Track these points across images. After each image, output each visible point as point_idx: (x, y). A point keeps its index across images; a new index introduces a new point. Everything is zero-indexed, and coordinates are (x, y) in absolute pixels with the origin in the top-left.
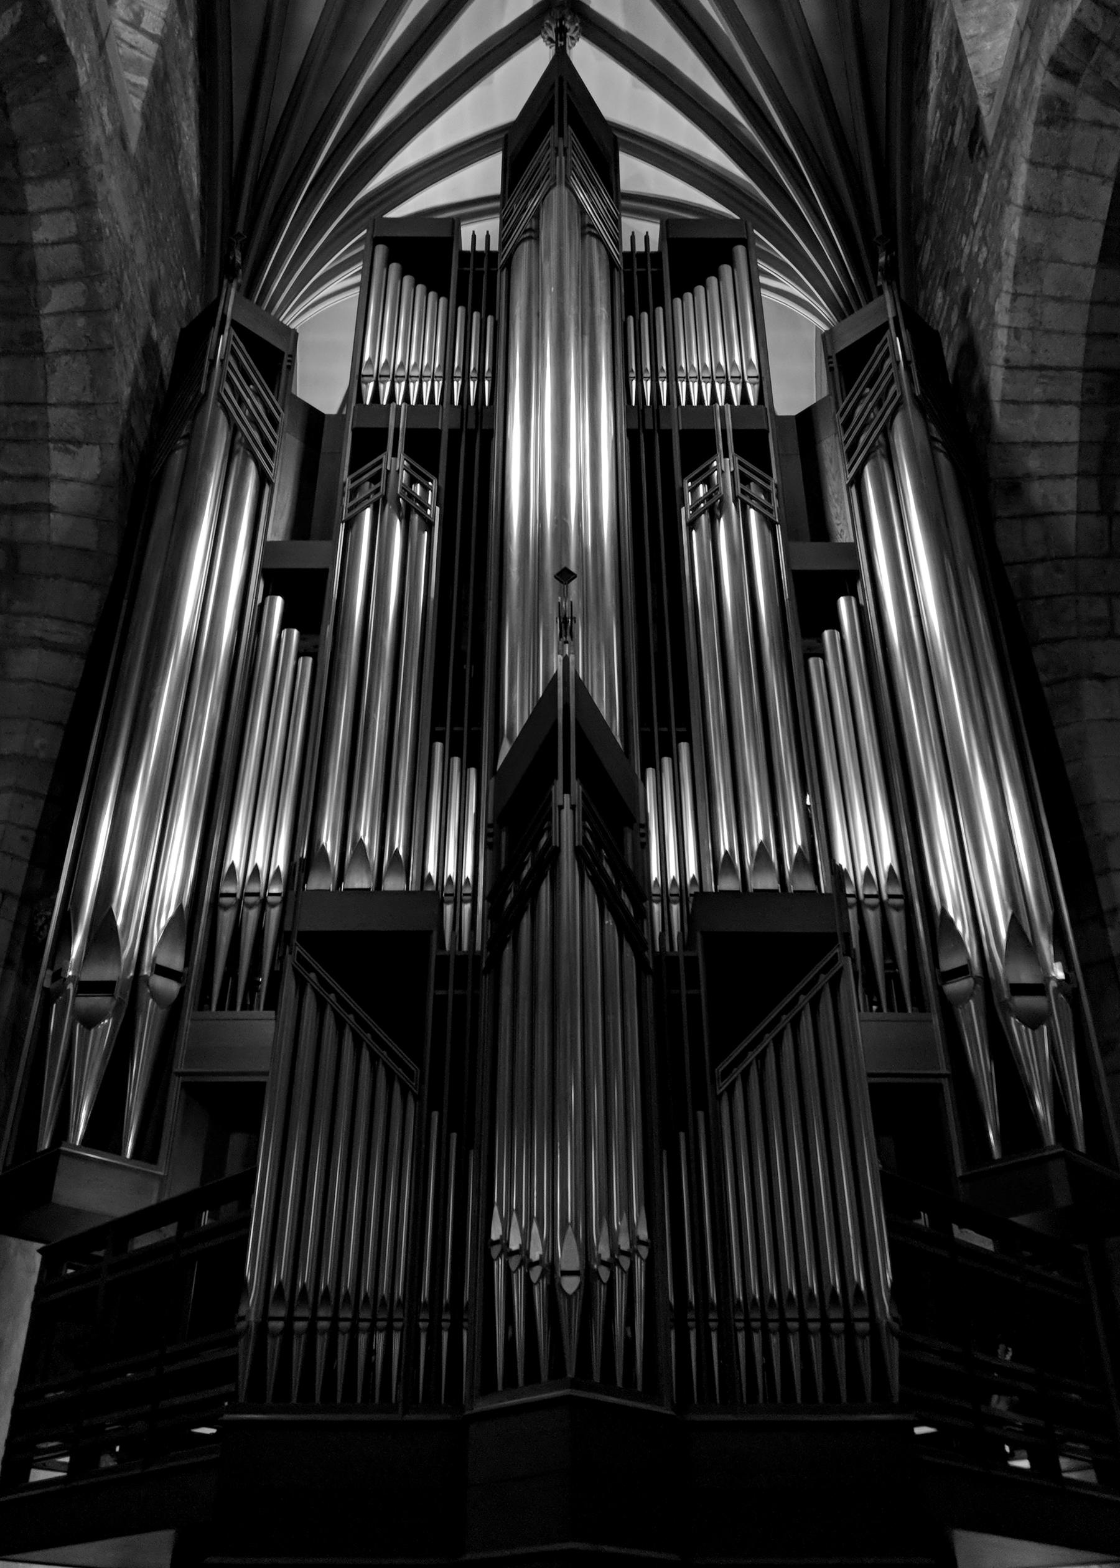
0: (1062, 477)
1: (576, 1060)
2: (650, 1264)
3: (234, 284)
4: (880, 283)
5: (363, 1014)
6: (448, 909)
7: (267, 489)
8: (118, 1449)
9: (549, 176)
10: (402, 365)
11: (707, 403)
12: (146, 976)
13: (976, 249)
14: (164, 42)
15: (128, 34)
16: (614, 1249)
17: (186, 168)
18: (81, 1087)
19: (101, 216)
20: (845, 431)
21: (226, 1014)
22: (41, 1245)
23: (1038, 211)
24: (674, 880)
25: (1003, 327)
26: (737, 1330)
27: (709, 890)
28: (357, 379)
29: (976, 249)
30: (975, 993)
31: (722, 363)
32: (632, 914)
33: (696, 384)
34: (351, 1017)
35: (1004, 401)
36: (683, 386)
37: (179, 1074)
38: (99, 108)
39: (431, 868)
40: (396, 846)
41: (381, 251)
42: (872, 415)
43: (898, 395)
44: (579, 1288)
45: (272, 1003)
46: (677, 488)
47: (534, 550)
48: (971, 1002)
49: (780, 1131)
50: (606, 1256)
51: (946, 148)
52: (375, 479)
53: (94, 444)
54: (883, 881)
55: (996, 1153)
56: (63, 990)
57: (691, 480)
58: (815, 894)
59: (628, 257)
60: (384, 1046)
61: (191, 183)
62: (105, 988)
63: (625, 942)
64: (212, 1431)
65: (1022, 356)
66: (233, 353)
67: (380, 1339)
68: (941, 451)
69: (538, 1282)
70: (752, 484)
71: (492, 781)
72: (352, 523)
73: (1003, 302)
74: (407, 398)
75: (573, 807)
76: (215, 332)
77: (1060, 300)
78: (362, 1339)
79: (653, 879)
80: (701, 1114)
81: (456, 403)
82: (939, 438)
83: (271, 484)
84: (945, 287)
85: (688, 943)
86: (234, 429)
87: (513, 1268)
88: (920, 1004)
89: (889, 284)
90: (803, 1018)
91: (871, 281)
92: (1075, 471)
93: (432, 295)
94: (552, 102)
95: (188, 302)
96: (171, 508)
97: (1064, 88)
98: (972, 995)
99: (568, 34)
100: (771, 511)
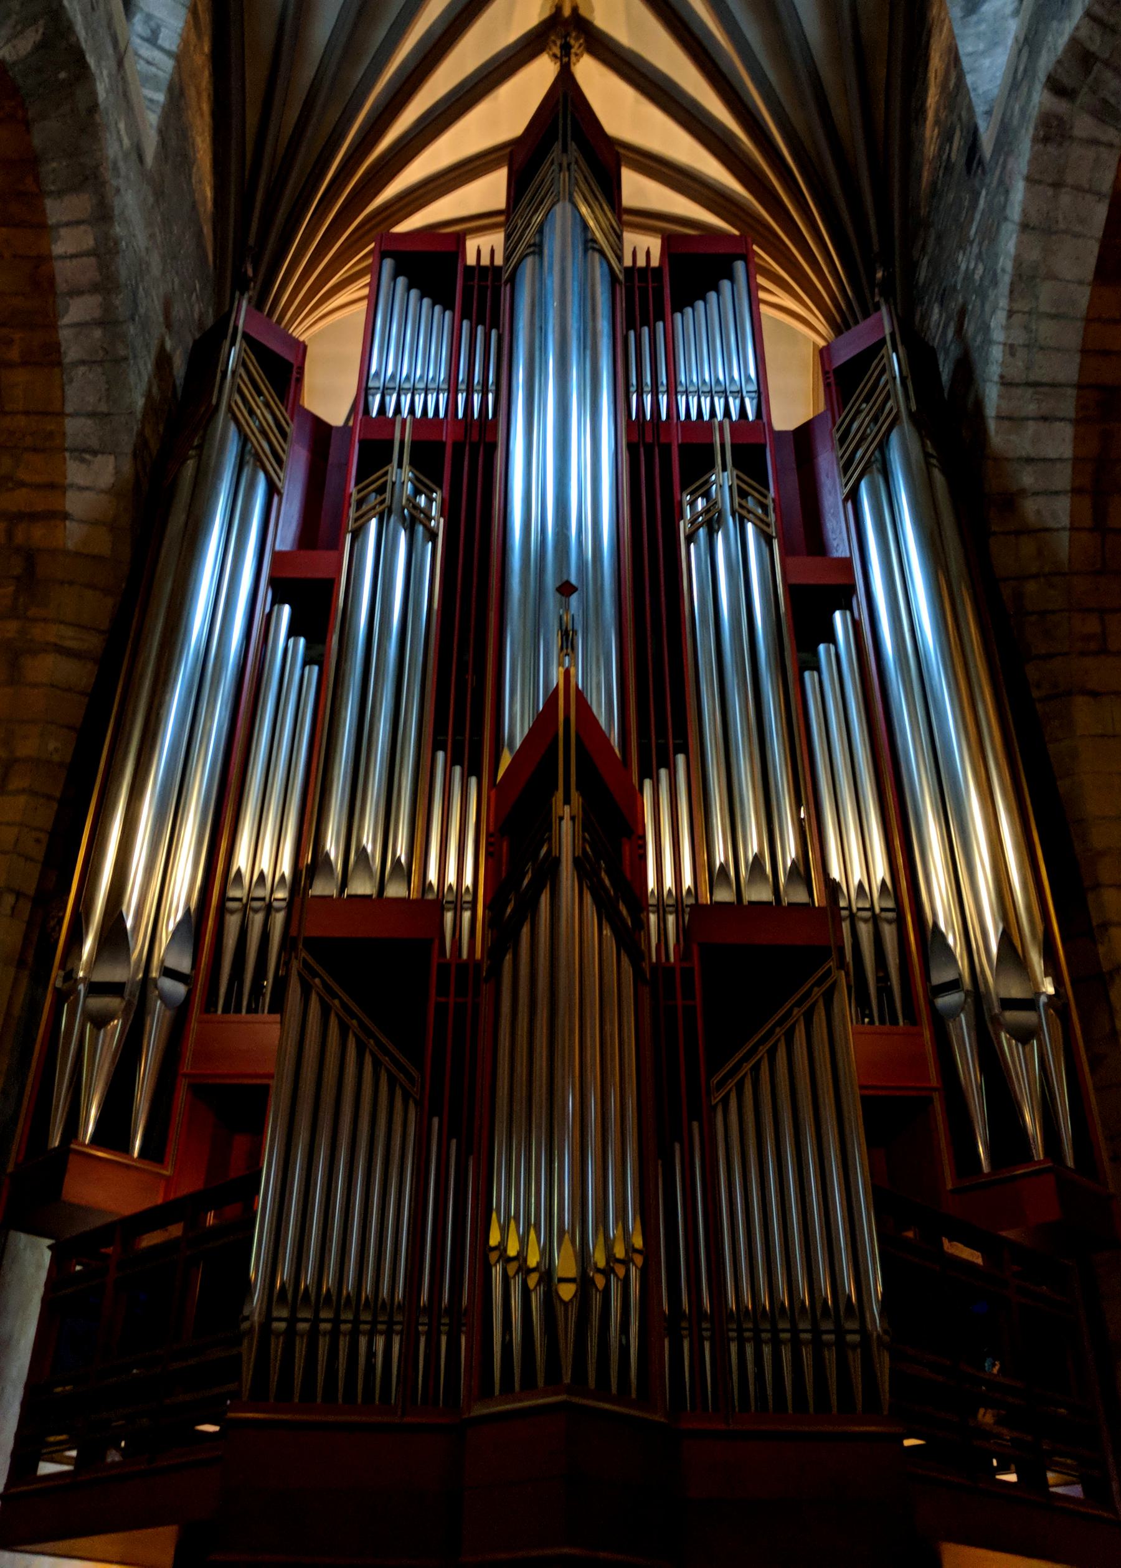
1: (574, 1066)
2: (644, 1272)
3: (246, 296)
4: (877, 299)
5: (367, 1021)
6: (449, 916)
8: (123, 1444)
10: (408, 378)
11: (706, 417)
12: (155, 978)
13: (972, 266)
14: (180, 58)
15: (146, 51)
16: (610, 1256)
17: (200, 182)
18: (90, 1088)
19: (118, 230)
20: (841, 447)
21: (232, 1017)
22: (49, 1242)
24: (670, 891)
25: (999, 343)
26: (730, 1339)
27: (705, 902)
28: (364, 391)
29: (972, 266)
30: (966, 1006)
31: (721, 378)
32: (630, 924)
33: (696, 399)
34: (354, 1022)
35: (999, 418)
36: (682, 401)
37: (186, 1075)
38: (116, 124)
39: (433, 876)
40: (398, 854)
41: (388, 264)
42: (868, 431)
43: (894, 411)
44: (575, 1295)
45: (277, 1006)
46: (675, 501)
47: (535, 565)
48: (962, 1016)
49: (773, 1142)
50: (602, 1264)
51: (944, 164)
52: (381, 490)
54: (876, 894)
56: (74, 991)
57: (691, 494)
58: (808, 907)
59: (629, 271)
60: (387, 1052)
61: (206, 198)
62: (114, 989)
63: (622, 952)
64: (216, 1428)
65: (1017, 371)
66: (244, 365)
67: (380, 1342)
68: (935, 466)
69: (535, 1287)
70: (749, 498)
71: (493, 792)
72: (359, 533)
75: (573, 818)
78: (363, 1341)
79: (650, 890)
80: (695, 1124)
81: (460, 415)
82: (935, 454)
83: (280, 494)
85: (684, 953)
86: (244, 440)
87: (511, 1273)
88: (911, 1016)
89: (887, 301)
90: (797, 1031)
91: (868, 296)
92: (1069, 488)
93: (437, 308)
95: (201, 315)
96: (183, 517)
97: (1062, 106)
98: (963, 1009)
99: (573, 51)
100: (768, 525)
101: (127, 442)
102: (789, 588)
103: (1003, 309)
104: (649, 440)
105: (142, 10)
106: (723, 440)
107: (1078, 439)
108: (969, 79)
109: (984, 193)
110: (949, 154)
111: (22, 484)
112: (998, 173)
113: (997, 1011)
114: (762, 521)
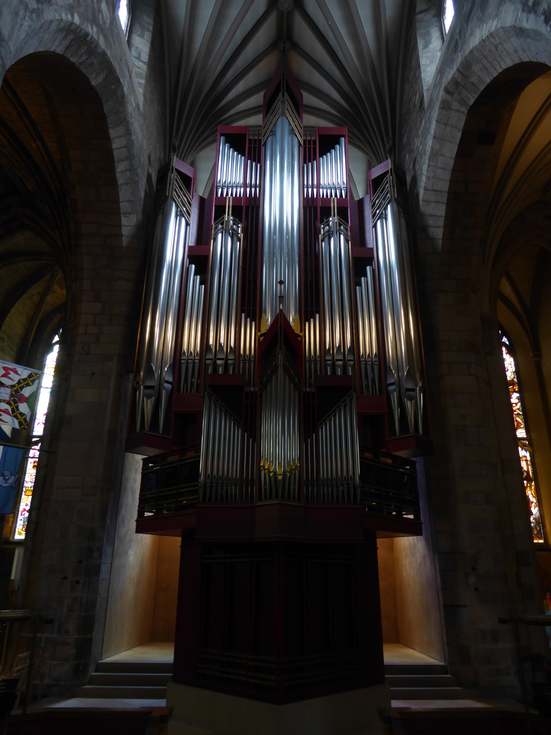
0: (439, 227)
7: (188, 227)
9: (279, 113)
13: (419, 145)
29: (419, 145)
36: (321, 190)
52: (222, 224)
53: (135, 214)
55: (398, 434)
72: (215, 240)
73: (425, 167)
76: (170, 172)
77: (443, 169)
83: (189, 225)
84: (409, 155)
86: (177, 207)
94: (280, 81)
101: (140, 209)
102: (354, 258)
103: (427, 164)
105: (134, 45)
106: (334, 205)
108: (423, 75)
109: (424, 120)
110: (415, 101)
112: (428, 115)
113: (404, 391)
114: (346, 235)
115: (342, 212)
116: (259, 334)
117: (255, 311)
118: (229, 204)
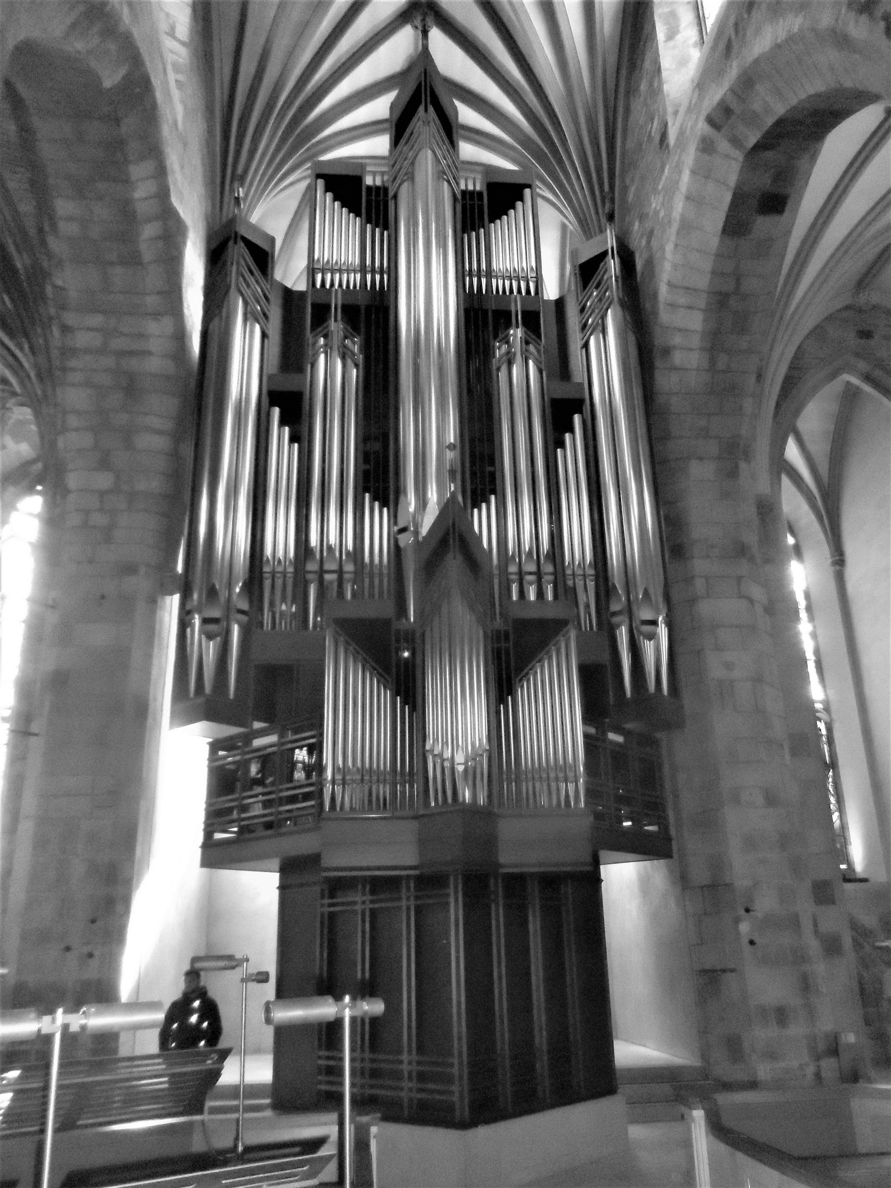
0: (691, 350)
7: (266, 341)
23: (693, 200)
36: (494, 281)
46: (491, 345)
59: (464, 193)
72: (313, 365)
74: (340, 285)
84: (640, 222)
86: (246, 303)
104: (476, 306)
107: (705, 320)
111: (122, 334)
115: (531, 320)
116: (396, 529)
117: (386, 489)
118: (337, 301)
